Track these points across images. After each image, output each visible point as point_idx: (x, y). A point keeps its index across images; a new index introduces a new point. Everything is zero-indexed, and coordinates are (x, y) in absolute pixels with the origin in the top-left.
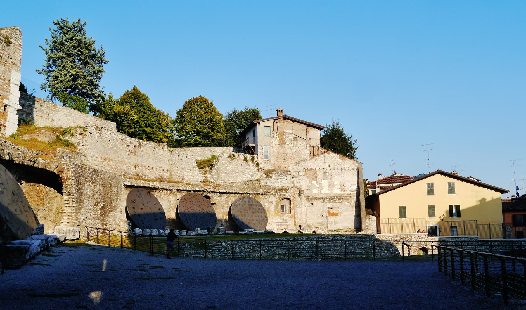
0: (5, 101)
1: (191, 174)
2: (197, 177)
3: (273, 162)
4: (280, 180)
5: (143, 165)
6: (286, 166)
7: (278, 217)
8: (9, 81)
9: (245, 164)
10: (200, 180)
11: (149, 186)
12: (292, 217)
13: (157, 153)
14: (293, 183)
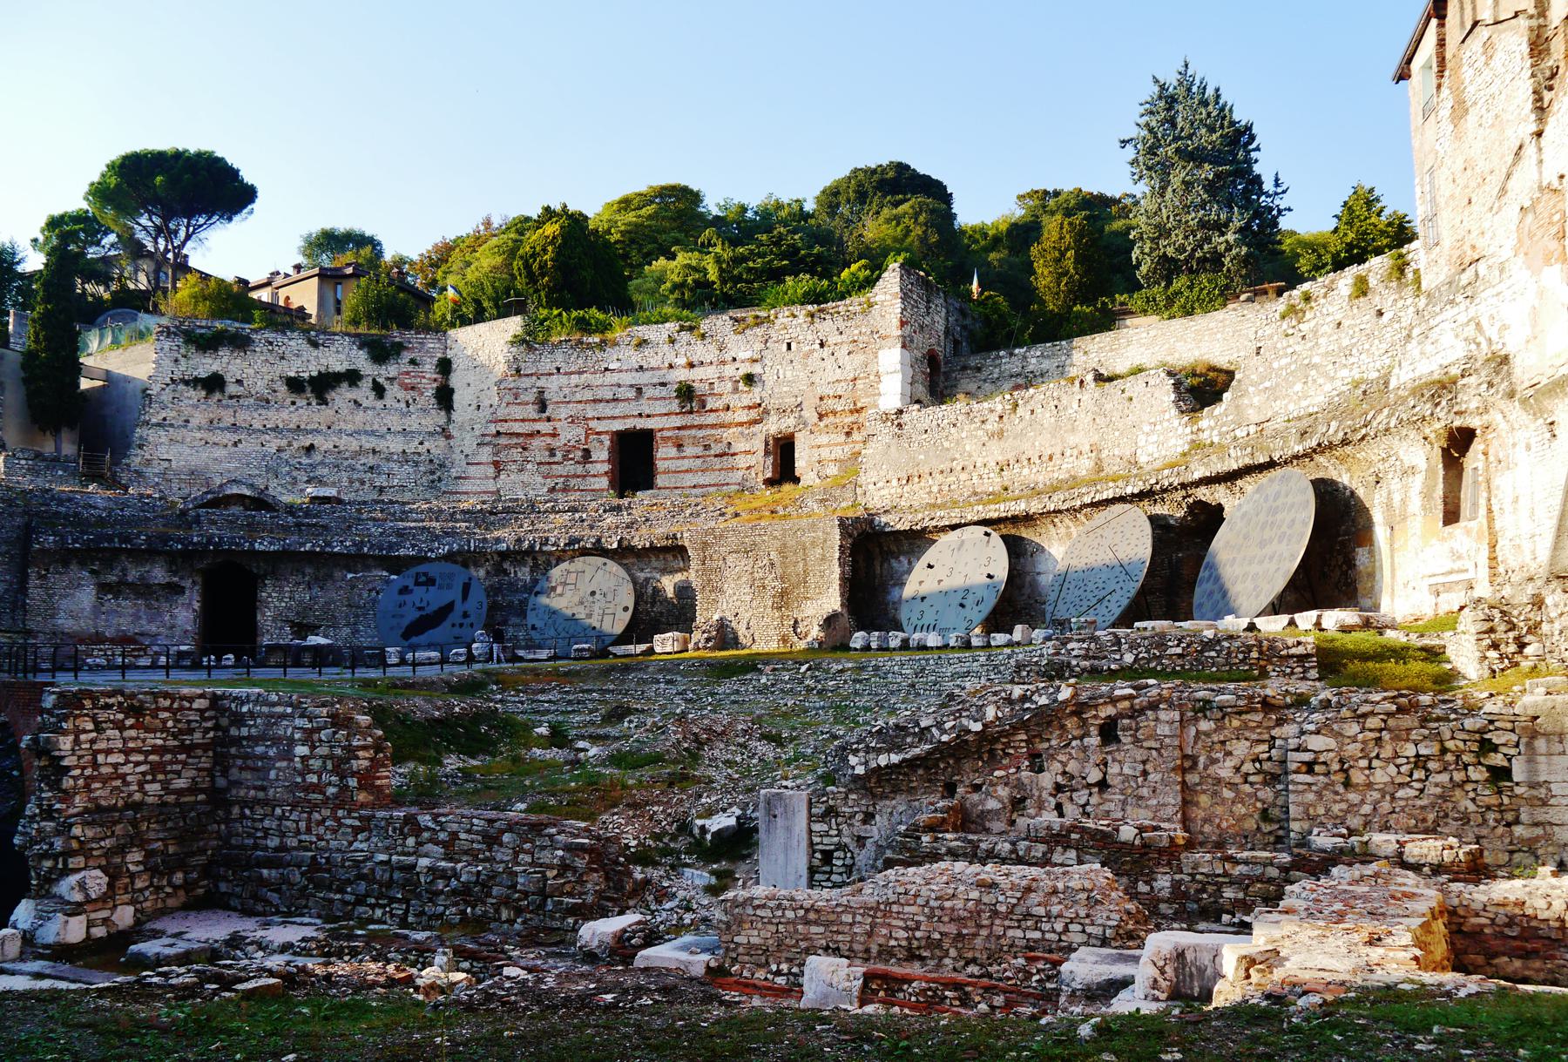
2: (1173, 442)
8: (877, 375)
9: (1362, 316)
10: (1180, 450)
11: (995, 515)
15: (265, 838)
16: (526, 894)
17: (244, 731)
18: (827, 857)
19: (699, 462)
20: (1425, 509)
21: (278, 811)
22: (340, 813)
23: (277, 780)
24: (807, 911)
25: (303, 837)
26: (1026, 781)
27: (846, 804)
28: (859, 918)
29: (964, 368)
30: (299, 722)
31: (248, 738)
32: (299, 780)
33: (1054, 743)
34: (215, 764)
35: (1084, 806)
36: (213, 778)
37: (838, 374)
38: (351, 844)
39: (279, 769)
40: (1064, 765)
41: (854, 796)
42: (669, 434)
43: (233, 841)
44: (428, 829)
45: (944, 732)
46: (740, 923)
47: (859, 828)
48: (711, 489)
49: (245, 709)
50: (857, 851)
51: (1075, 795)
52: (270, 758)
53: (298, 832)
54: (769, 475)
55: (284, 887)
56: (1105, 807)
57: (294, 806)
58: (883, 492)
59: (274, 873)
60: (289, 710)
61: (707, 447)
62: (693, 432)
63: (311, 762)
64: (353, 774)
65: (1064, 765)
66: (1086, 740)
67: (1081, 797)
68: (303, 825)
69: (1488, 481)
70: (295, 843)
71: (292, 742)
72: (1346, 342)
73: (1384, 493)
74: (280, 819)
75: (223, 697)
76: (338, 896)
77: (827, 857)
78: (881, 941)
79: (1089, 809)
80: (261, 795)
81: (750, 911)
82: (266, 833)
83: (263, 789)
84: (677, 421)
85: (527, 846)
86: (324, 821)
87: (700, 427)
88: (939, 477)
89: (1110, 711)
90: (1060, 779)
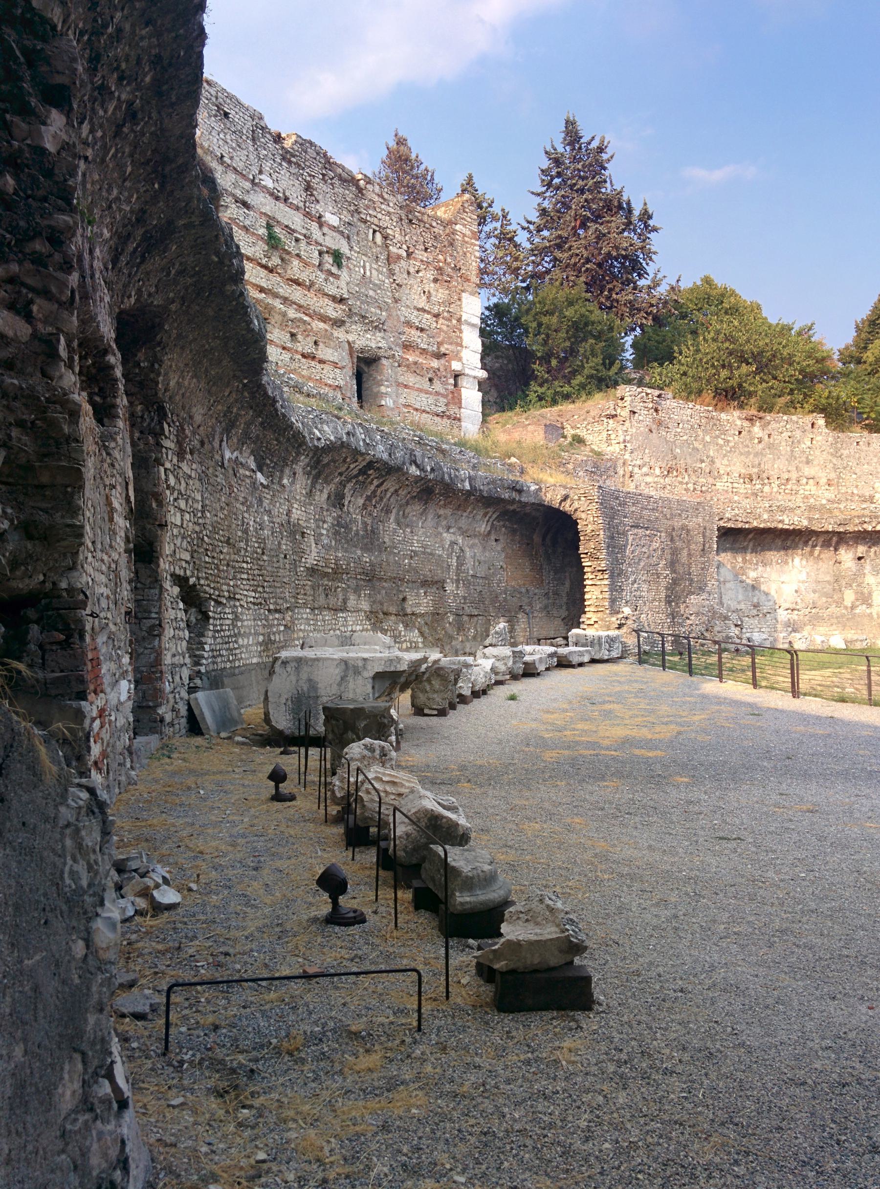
0: (456, 366)
5: (765, 475)
8: (459, 320)
13: (799, 442)
37: (422, 303)
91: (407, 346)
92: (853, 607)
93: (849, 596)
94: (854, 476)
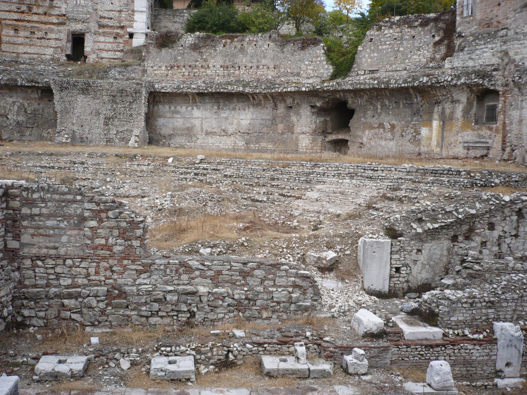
0: (129, 30)
1: (311, 67)
2: (322, 71)
3: (478, 16)
4: (478, 52)
6: (500, 18)
7: (470, 132)
12: (497, 131)
13: (260, 47)
14: (506, 53)
15: (58, 279)
16: (278, 303)
17: (36, 211)
18: (398, 270)
19: (27, 40)
20: (463, 116)
21: (69, 262)
22: (125, 262)
23: (69, 242)
24: (487, 303)
25: (92, 278)
26: (488, 234)
27: (409, 246)
28: (510, 304)
29: (166, 14)
30: (87, 205)
31: (39, 215)
32: (89, 242)
33: (498, 218)
34: (6, 231)
35: (508, 244)
36: (5, 241)
37: (111, 7)
38: (135, 280)
39: (71, 236)
40: (503, 227)
41: (413, 242)
42: (10, 22)
43: (27, 282)
44: (198, 269)
45: (459, 213)
46: (455, 311)
47: (414, 256)
48: (35, 56)
49: (36, 196)
50: (412, 266)
51: (506, 240)
52: (62, 228)
53: (88, 275)
54: (69, 52)
55: (85, 310)
56: (517, 245)
57: (83, 259)
58: (156, 72)
59: (73, 301)
60: (79, 198)
61: (33, 33)
62: (25, 24)
63: (99, 231)
64: (137, 238)
65: (503, 227)
66: (512, 217)
67: (508, 241)
68: (92, 270)
69: (505, 112)
70: (85, 281)
71: (83, 219)
72: (417, 44)
73: (440, 108)
74: (71, 267)
75: (12, 186)
76: (133, 313)
77: (398, 270)
78: (518, 313)
79: (511, 245)
80: (52, 252)
81: (460, 305)
82: (58, 276)
83: (56, 248)
84: (16, 16)
85: (270, 276)
86: (111, 267)
87: (29, 21)
88: (190, 70)
89: (520, 206)
90: (501, 234)
91: (103, 26)
92: (283, 133)
93: (281, 127)
94: (289, 62)
